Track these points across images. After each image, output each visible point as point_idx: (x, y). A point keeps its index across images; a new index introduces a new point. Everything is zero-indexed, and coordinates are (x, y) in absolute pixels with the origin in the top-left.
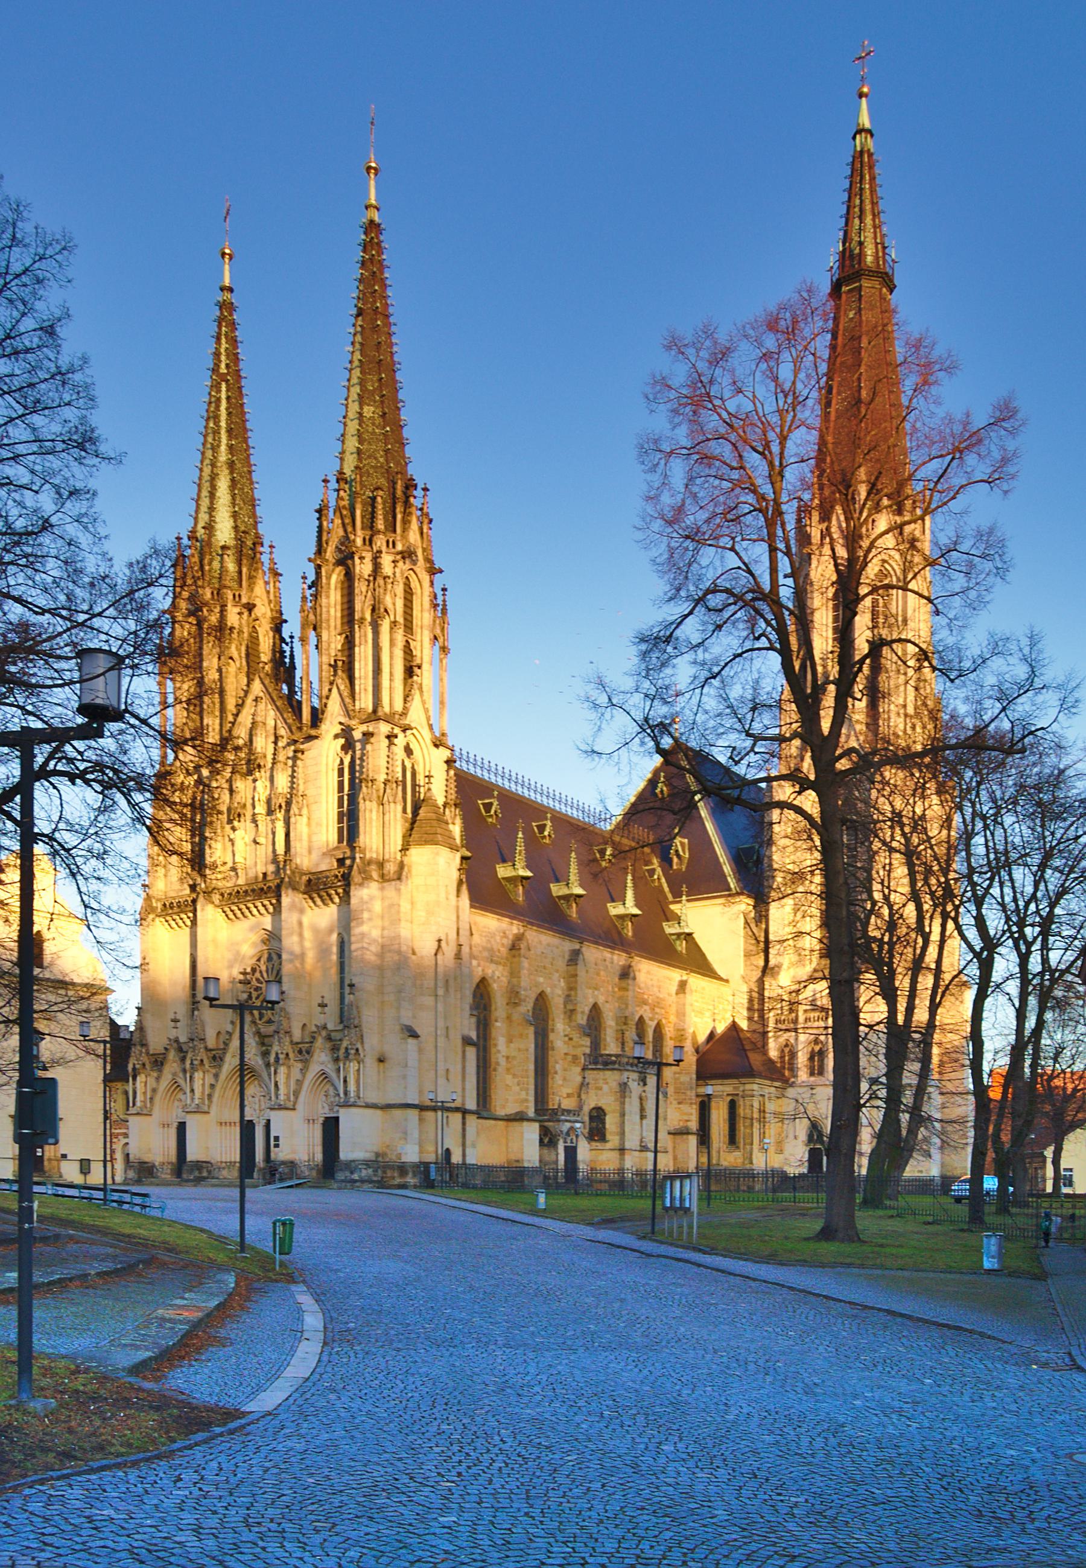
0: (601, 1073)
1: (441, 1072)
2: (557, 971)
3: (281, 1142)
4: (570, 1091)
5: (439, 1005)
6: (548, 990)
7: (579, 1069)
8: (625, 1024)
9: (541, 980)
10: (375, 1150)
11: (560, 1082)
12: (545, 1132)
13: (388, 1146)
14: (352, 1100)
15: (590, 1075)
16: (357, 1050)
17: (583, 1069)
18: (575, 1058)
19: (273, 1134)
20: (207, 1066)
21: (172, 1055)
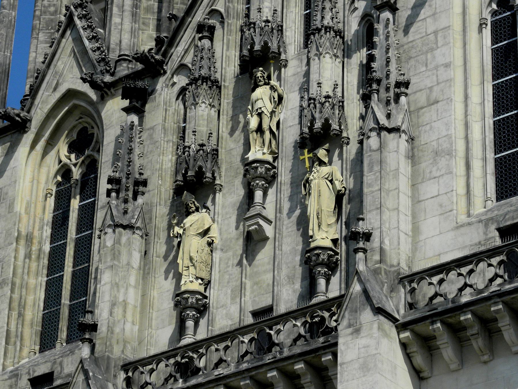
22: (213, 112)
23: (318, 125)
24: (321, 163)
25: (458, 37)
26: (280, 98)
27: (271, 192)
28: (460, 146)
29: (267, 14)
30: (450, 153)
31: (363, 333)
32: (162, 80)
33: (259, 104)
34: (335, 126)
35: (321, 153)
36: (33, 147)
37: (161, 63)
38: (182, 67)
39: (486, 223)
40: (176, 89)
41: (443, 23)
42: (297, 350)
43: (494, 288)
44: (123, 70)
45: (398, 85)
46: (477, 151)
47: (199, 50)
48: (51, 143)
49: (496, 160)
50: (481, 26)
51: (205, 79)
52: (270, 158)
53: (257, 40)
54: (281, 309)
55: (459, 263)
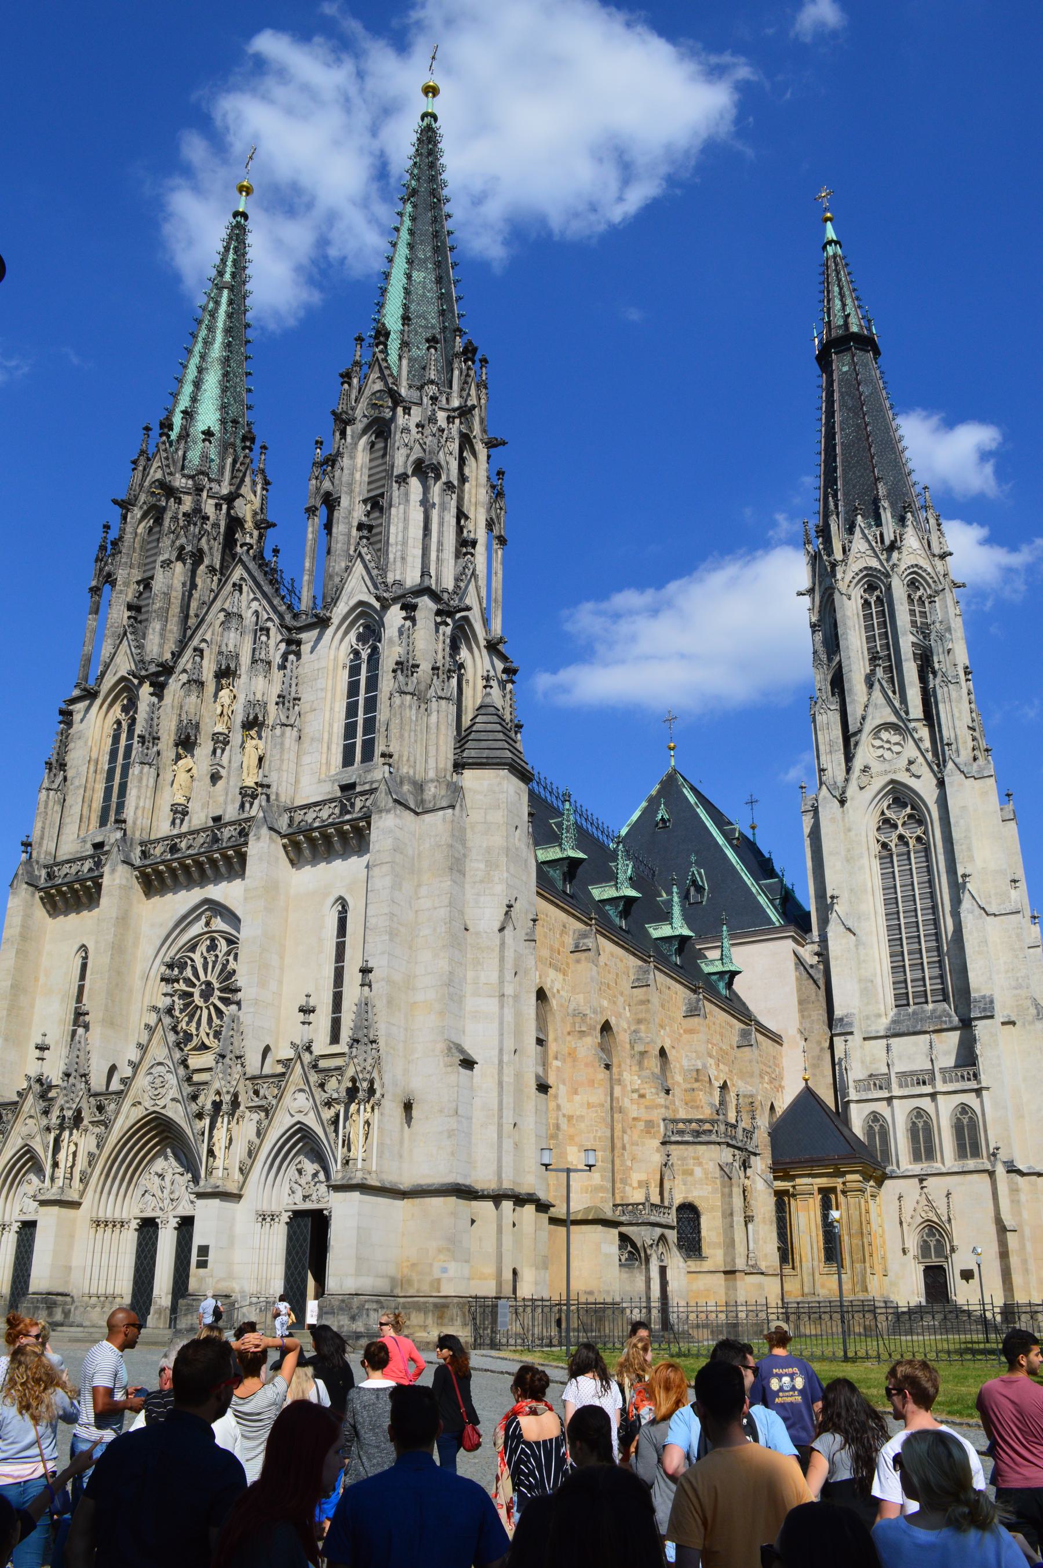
0: (691, 1148)
1: (508, 1127)
2: (622, 994)
3: (211, 1257)
4: (643, 1177)
5: (506, 1010)
6: (613, 1022)
7: (656, 1143)
8: (697, 1080)
9: (605, 1003)
10: (392, 1271)
11: (629, 1163)
12: (624, 1238)
13: (413, 1265)
14: (359, 1174)
15: (675, 1151)
16: (372, 1082)
17: (663, 1143)
18: (650, 1124)
19: (197, 1241)
20: (85, 1122)
21: (31, 1104)
22: (199, 700)
23: (251, 717)
24: (252, 738)
25: (331, 673)
26: (235, 697)
27: (228, 748)
28: (326, 736)
29: (231, 648)
30: (321, 741)
31: (262, 840)
32: (174, 676)
33: (223, 700)
34: (261, 718)
35: (253, 733)
36: (101, 707)
37: (173, 668)
38: (184, 671)
39: (333, 782)
40: (180, 683)
41: (323, 664)
42: (230, 844)
43: (330, 820)
44: (153, 669)
45: (295, 699)
46: (335, 739)
47: (194, 663)
48: (111, 706)
49: (345, 745)
50: (344, 667)
51: (195, 681)
52: (226, 732)
53: (224, 662)
54: (227, 818)
55: (316, 804)
